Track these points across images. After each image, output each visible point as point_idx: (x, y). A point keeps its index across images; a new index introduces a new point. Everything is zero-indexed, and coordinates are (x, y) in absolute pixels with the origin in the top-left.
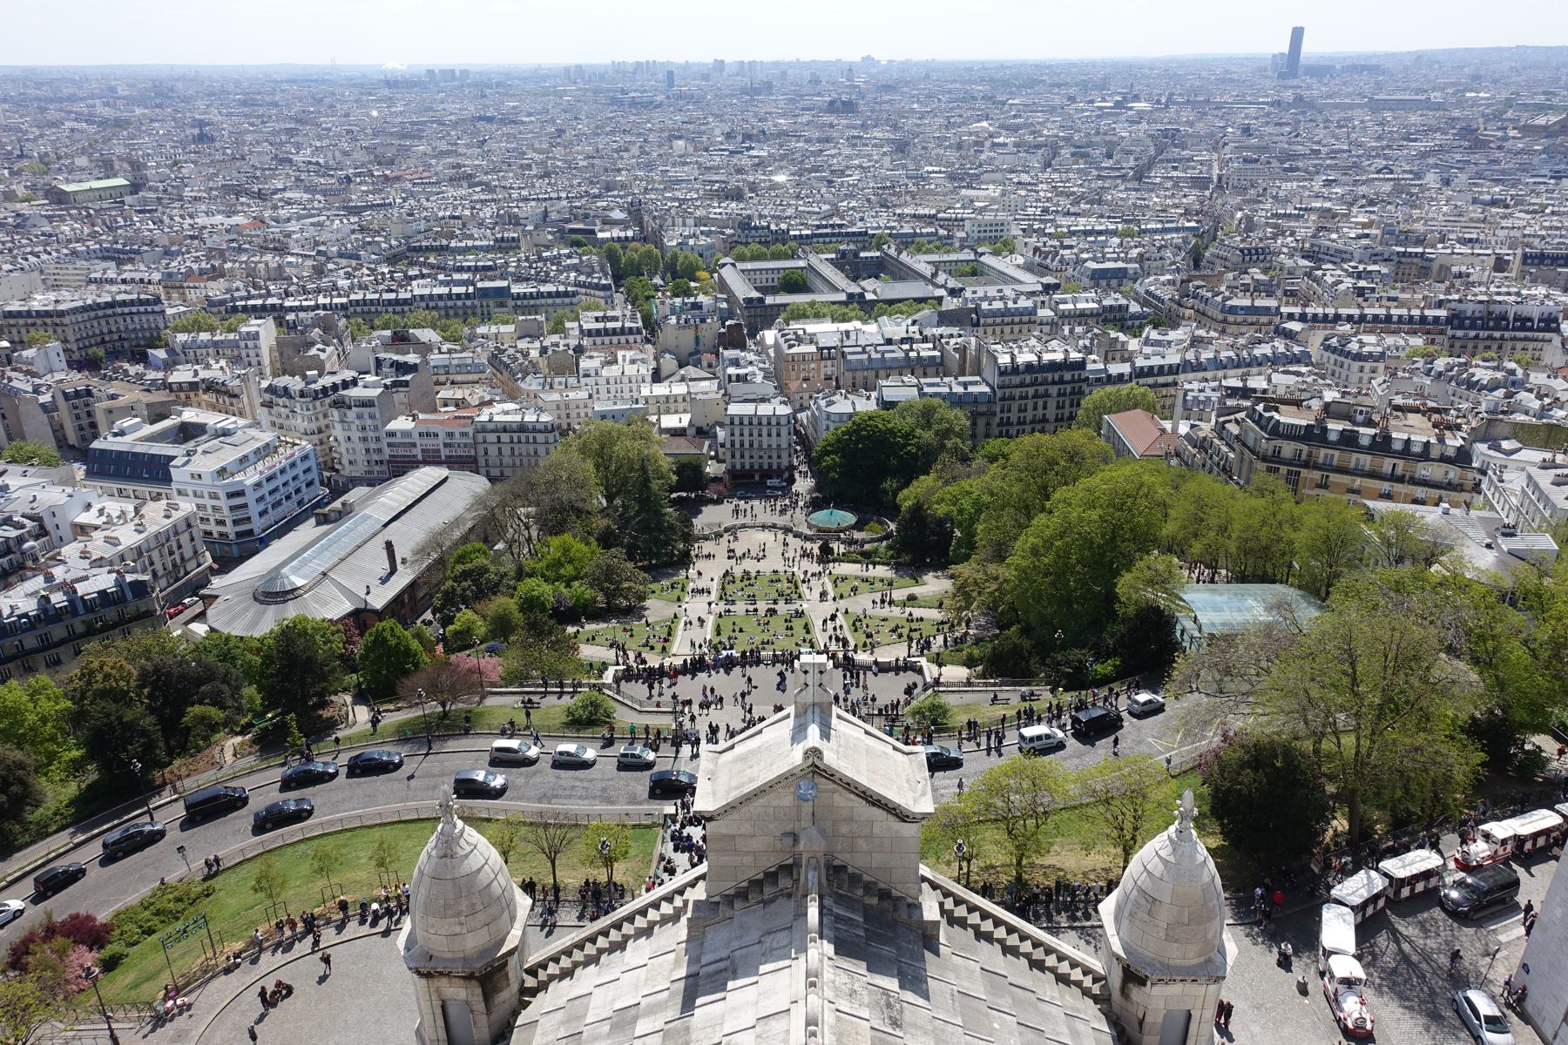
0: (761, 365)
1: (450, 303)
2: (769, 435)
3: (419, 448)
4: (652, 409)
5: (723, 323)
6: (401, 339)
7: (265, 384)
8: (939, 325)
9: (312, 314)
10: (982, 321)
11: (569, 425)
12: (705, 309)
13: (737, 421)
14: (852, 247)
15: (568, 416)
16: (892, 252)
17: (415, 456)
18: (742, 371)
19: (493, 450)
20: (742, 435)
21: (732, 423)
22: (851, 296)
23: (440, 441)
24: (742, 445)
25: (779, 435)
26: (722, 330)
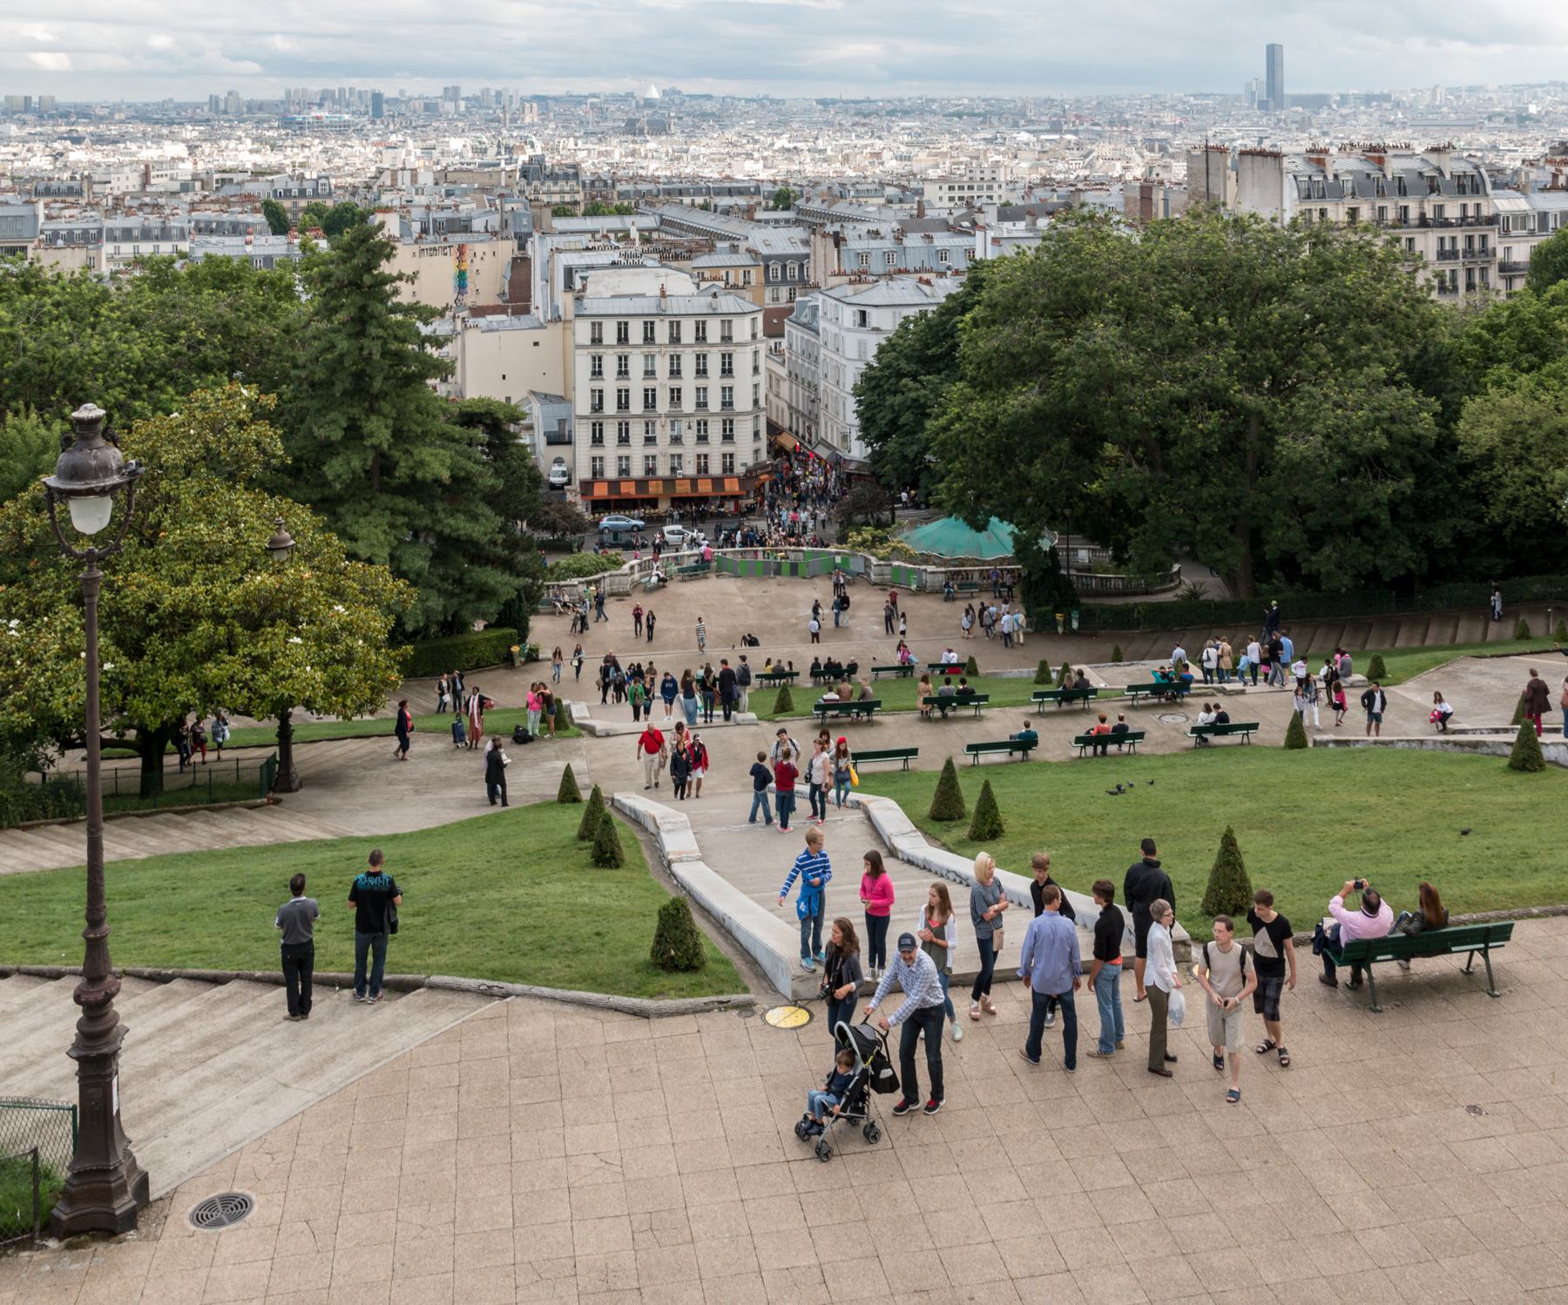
2: (702, 372)
12: (478, 225)
20: (623, 373)
21: (597, 341)
24: (623, 402)
25: (727, 371)
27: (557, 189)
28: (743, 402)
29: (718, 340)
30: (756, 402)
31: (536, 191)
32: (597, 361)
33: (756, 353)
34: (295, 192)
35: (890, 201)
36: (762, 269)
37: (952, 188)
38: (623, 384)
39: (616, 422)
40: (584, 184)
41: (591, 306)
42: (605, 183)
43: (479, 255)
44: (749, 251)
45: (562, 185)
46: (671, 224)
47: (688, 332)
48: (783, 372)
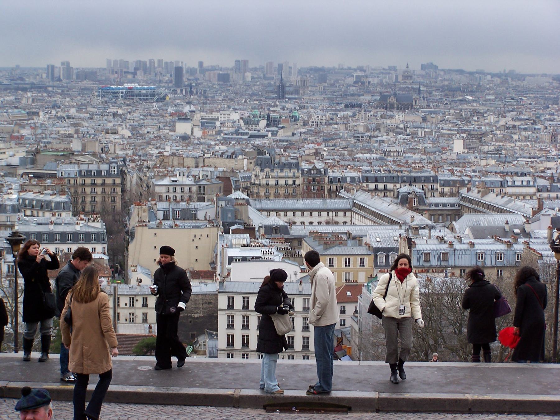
12: (201, 215)
13: (238, 303)
20: (245, 326)
21: (231, 306)
27: (283, 174)
29: (302, 310)
31: (267, 177)
32: (231, 318)
35: (539, 190)
36: (372, 256)
38: (245, 332)
39: (241, 353)
40: (303, 171)
41: (229, 287)
42: (319, 171)
44: (367, 244)
45: (287, 172)
48: (356, 327)
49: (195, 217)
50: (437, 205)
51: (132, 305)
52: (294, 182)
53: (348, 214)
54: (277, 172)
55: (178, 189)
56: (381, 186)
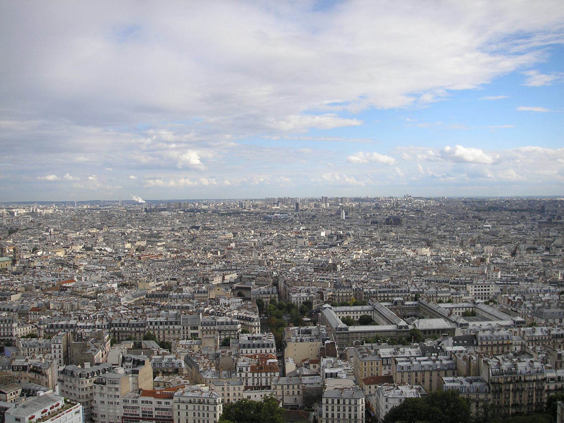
0: (346, 368)
1: (166, 327)
2: (350, 410)
3: (141, 410)
4: (279, 393)
5: (324, 342)
6: (138, 346)
7: (61, 368)
8: (454, 345)
9: (91, 330)
10: (480, 343)
11: (228, 400)
12: (313, 333)
13: (330, 401)
14: (401, 299)
15: (228, 395)
16: (424, 301)
17: (139, 415)
18: (334, 371)
19: (183, 414)
20: (333, 410)
21: (327, 402)
22: (401, 327)
23: (155, 405)
24: (333, 416)
25: (356, 411)
26: (322, 346)
28: (359, 417)
30: (362, 417)
32: (327, 407)
33: (363, 406)
34: (266, 292)
35: (452, 294)
36: (381, 362)
37: (475, 287)
38: (333, 412)
40: (353, 289)
43: (312, 345)
46: (376, 309)
47: (347, 402)
49: (310, 333)
50: (409, 305)
51: (288, 388)
52: (350, 294)
53: (372, 312)
54: (343, 290)
55: (302, 298)
56: (386, 295)
